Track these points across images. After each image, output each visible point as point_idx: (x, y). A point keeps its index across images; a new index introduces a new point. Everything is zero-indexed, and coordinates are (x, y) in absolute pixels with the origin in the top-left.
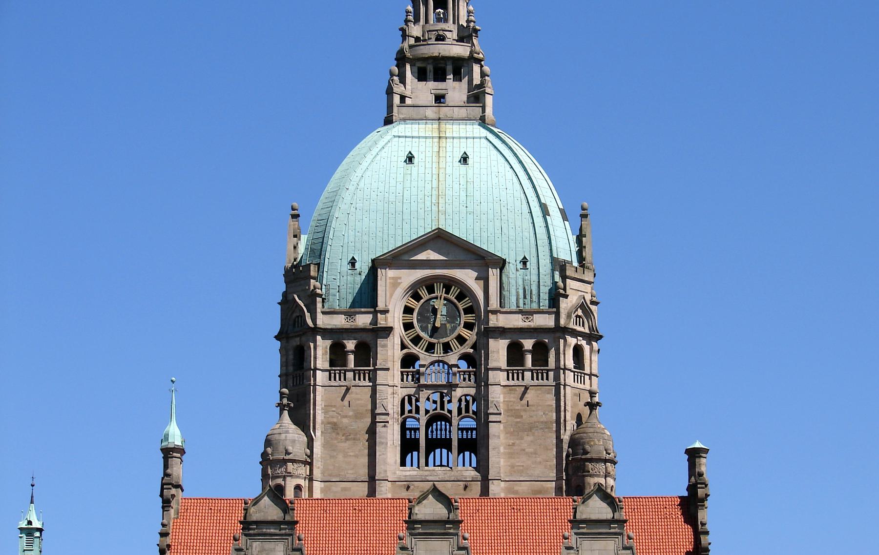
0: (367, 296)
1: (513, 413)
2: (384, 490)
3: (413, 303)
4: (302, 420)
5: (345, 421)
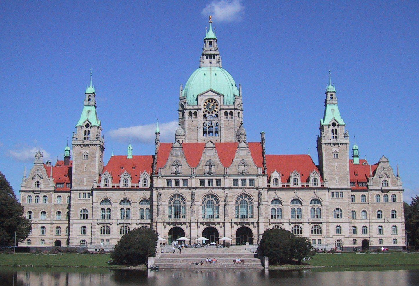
1: (226, 126)
3: (205, 104)
4: (183, 128)
5: (192, 127)
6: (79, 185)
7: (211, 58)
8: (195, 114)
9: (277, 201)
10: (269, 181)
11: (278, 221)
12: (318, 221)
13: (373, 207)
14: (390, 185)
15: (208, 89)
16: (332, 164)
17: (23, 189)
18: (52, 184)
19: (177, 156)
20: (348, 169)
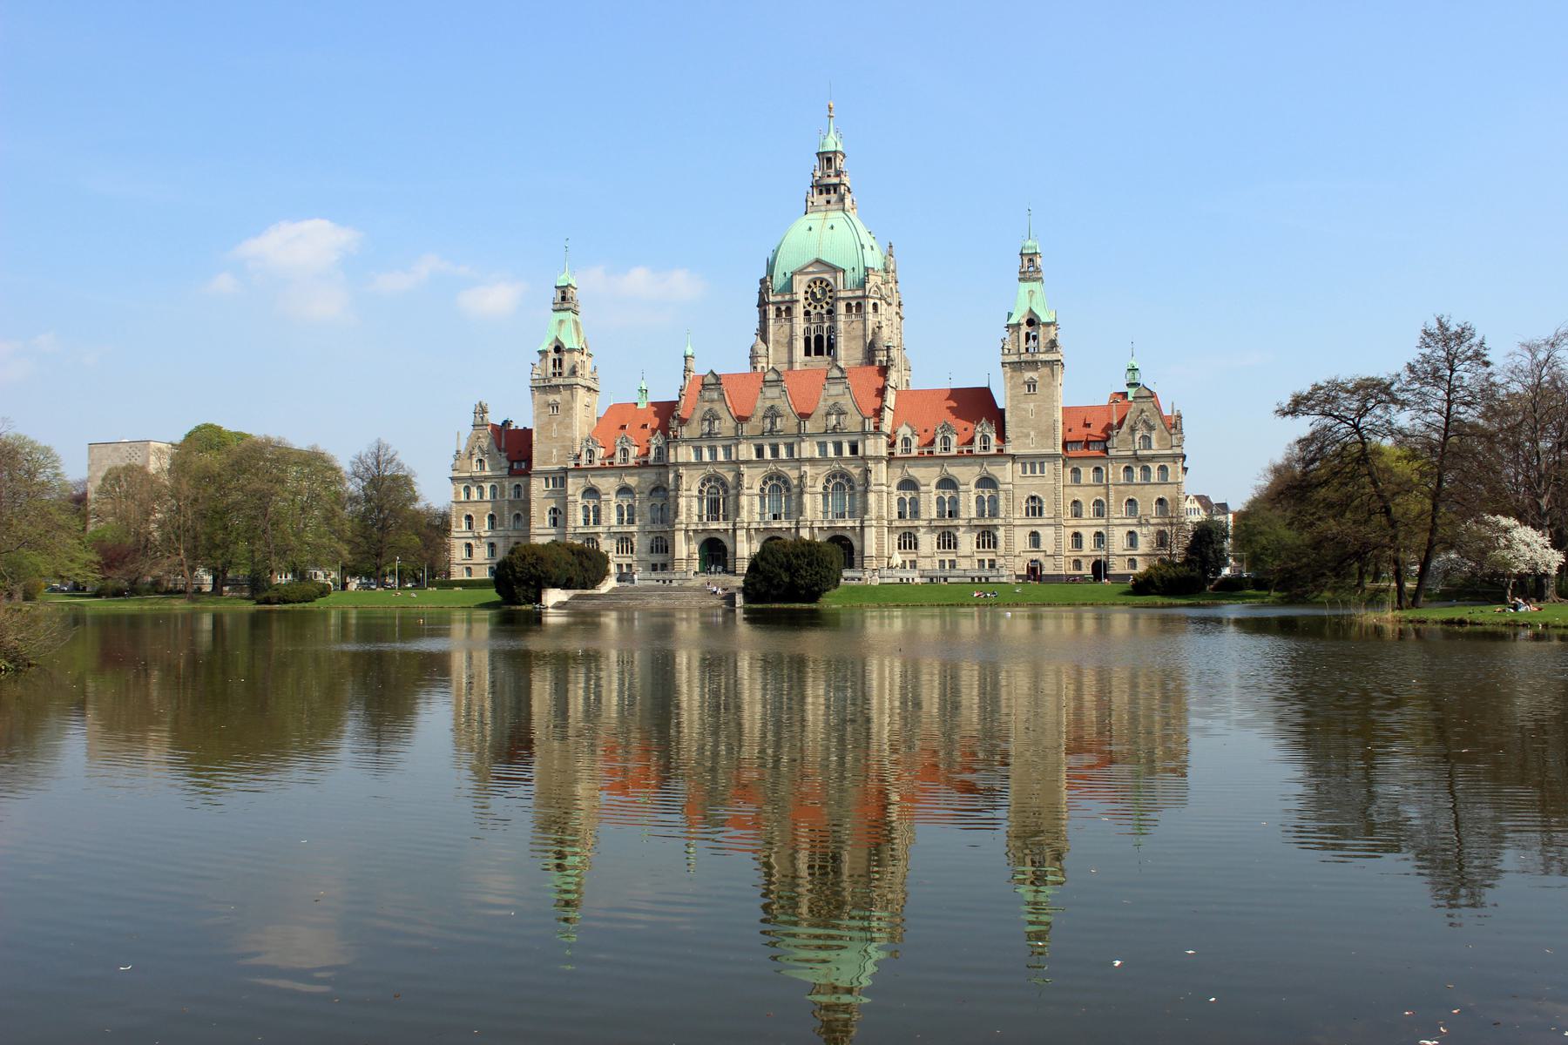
0: (789, 287)
2: (797, 367)
6: (545, 463)
7: (828, 192)
8: (789, 310)
9: (908, 484)
10: (892, 445)
11: (910, 523)
12: (988, 522)
13: (1117, 492)
14: (1154, 445)
15: (812, 258)
16: (1024, 406)
17: (456, 474)
18: (505, 463)
19: (712, 401)
20: (1059, 416)
